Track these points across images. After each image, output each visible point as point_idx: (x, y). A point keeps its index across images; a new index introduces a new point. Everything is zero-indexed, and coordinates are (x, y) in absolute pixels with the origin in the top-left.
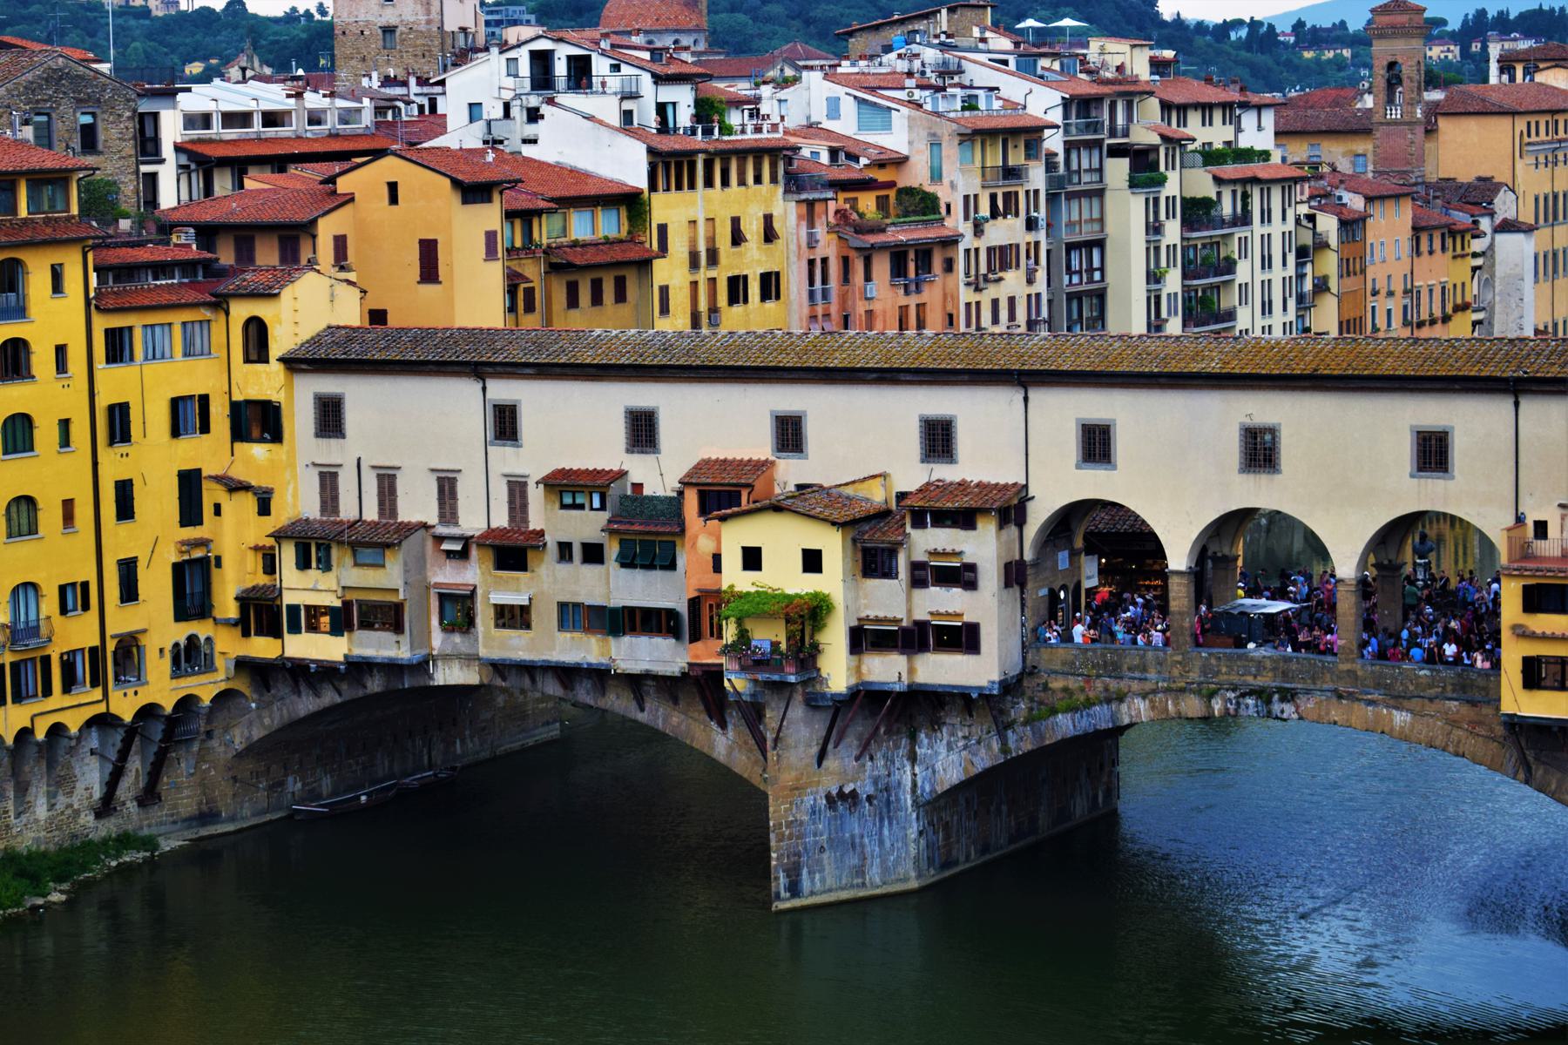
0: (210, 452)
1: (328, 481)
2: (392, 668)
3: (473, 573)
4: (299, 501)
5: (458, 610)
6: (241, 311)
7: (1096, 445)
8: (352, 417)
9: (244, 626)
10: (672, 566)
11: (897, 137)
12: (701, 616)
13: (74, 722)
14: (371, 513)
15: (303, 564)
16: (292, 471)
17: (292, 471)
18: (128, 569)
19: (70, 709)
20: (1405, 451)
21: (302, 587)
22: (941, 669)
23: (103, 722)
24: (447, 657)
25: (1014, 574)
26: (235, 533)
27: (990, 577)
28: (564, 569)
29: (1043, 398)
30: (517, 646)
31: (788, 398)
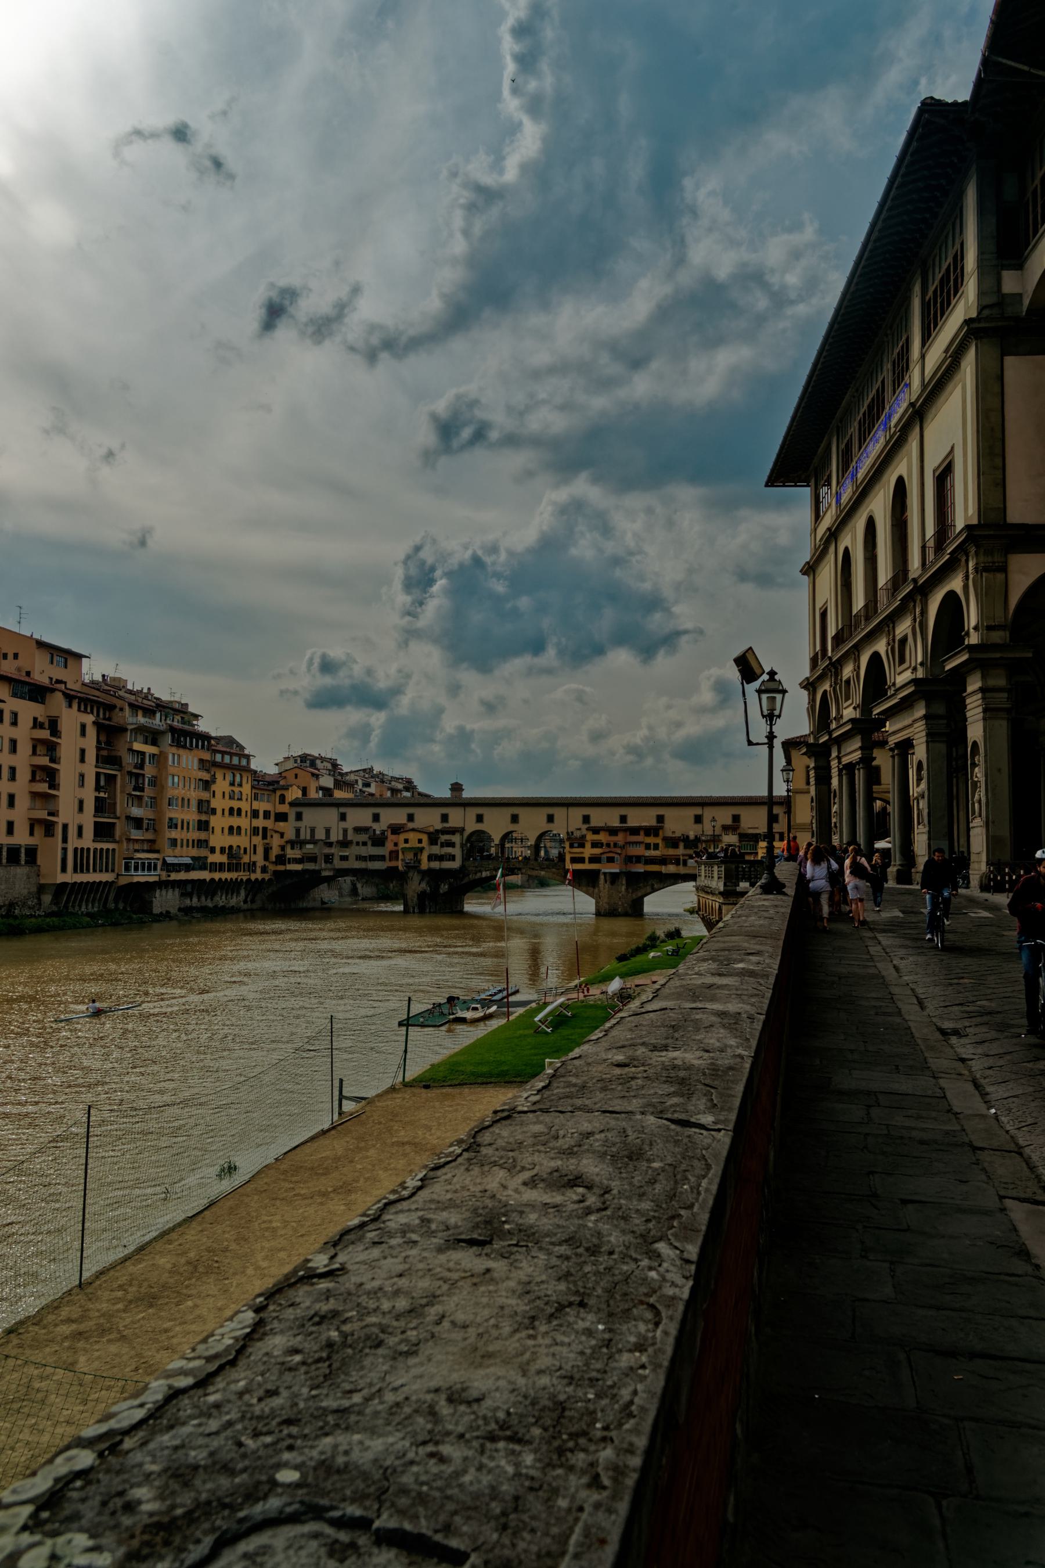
0: (269, 824)
1: (298, 831)
2: (314, 871)
3: (333, 850)
4: (290, 835)
5: (328, 859)
6: (278, 793)
7: (480, 819)
8: (304, 816)
9: (276, 863)
10: (383, 845)
11: (372, 790)
12: (394, 855)
13: (245, 879)
14: (308, 838)
15: (292, 848)
16: (288, 828)
17: (288, 828)
18: (255, 846)
19: (242, 875)
20: (545, 818)
21: (290, 853)
22: (447, 865)
23: (249, 880)
24: (325, 869)
25: (462, 845)
26: (276, 842)
27: (458, 845)
28: (357, 848)
29: (468, 809)
30: (345, 865)
31: (411, 810)
